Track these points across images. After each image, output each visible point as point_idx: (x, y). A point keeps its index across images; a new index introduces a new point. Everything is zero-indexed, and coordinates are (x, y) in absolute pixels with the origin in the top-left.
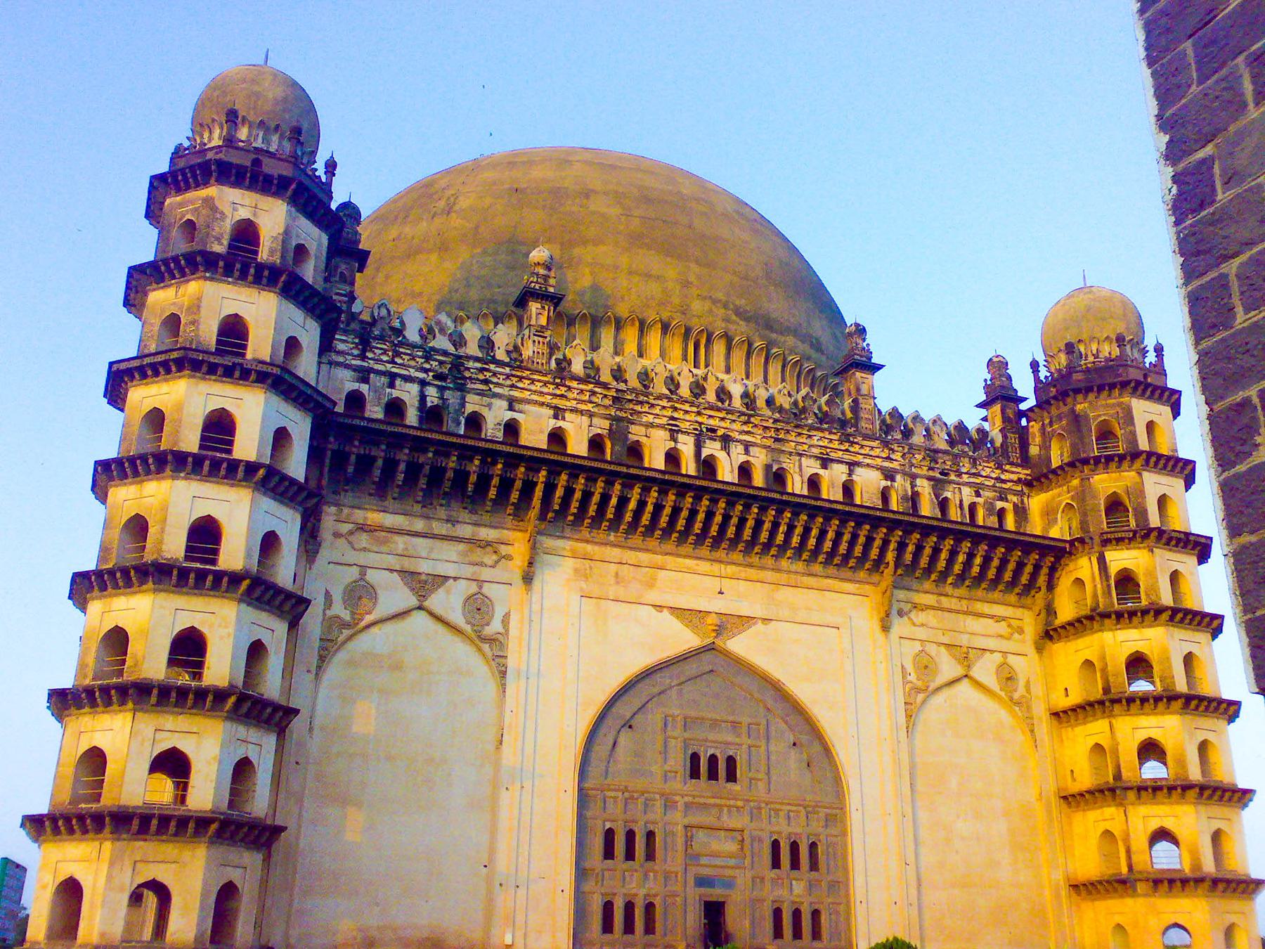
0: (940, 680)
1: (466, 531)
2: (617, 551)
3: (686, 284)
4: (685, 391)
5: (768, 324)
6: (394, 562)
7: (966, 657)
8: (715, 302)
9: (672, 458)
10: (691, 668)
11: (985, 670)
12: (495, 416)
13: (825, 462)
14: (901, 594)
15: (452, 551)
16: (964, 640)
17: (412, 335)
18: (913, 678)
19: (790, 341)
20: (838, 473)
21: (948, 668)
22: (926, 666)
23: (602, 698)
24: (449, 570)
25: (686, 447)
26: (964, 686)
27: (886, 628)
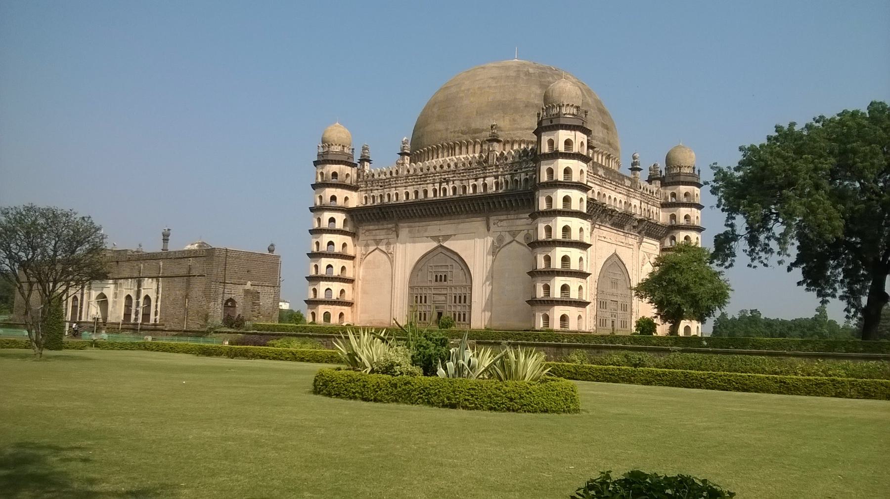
0: (505, 243)
1: (385, 226)
2: (417, 224)
3: (447, 129)
4: (438, 169)
5: (477, 131)
6: (372, 238)
7: (514, 234)
8: (455, 132)
9: (435, 191)
10: (436, 252)
11: (520, 238)
12: (393, 192)
13: (476, 179)
14: (495, 218)
15: (383, 232)
16: (514, 228)
17: (376, 176)
18: (496, 244)
19: (484, 133)
20: (481, 181)
21: (508, 238)
22: (500, 240)
23: (414, 264)
24: (382, 237)
25: (437, 186)
26: (514, 243)
27: (488, 230)
